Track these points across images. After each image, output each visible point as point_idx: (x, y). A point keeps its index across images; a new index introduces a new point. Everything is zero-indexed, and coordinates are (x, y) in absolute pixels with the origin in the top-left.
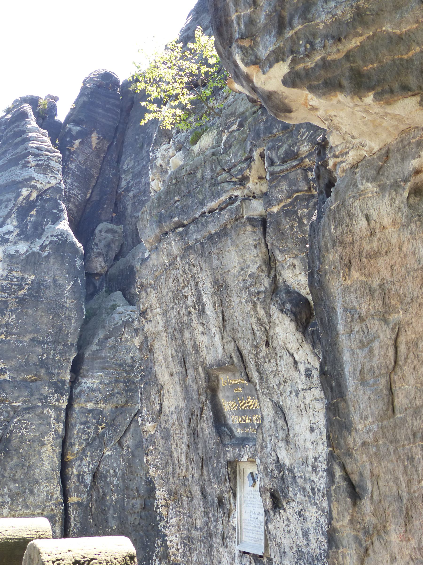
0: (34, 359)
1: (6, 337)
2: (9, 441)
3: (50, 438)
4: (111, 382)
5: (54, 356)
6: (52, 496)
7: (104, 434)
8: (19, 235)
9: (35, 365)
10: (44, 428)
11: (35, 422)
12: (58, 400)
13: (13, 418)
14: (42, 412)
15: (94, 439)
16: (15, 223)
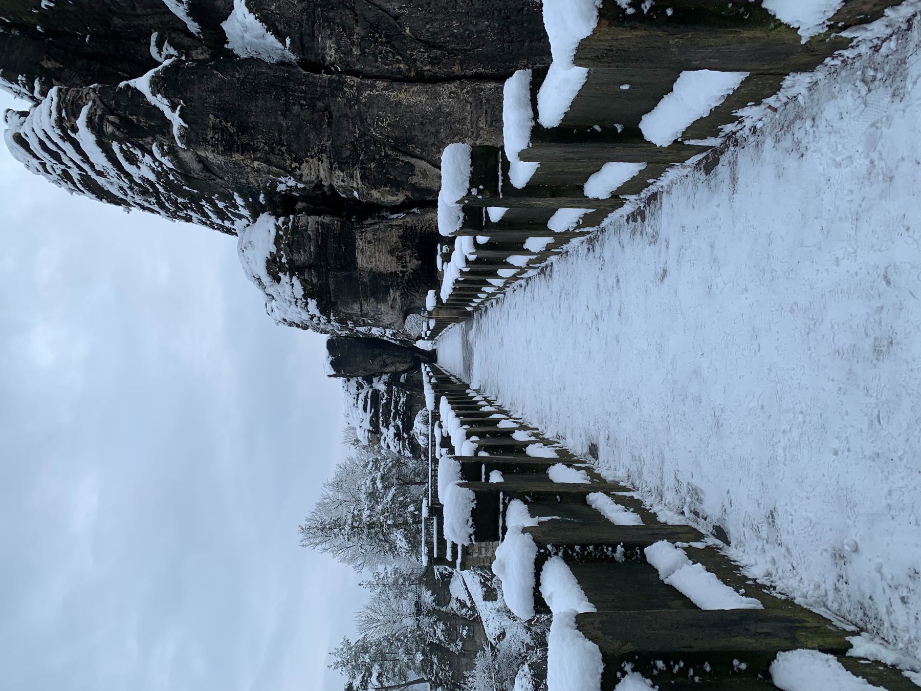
0: (306, 114)
1: (283, 145)
2: (396, 139)
3: (392, 95)
4: (329, 26)
5: (302, 92)
6: (453, 93)
7: (387, 36)
8: (163, 134)
9: (313, 113)
10: (382, 103)
11: (375, 112)
12: (351, 87)
13: (372, 136)
14: (365, 104)
15: (392, 46)
16: (149, 139)
